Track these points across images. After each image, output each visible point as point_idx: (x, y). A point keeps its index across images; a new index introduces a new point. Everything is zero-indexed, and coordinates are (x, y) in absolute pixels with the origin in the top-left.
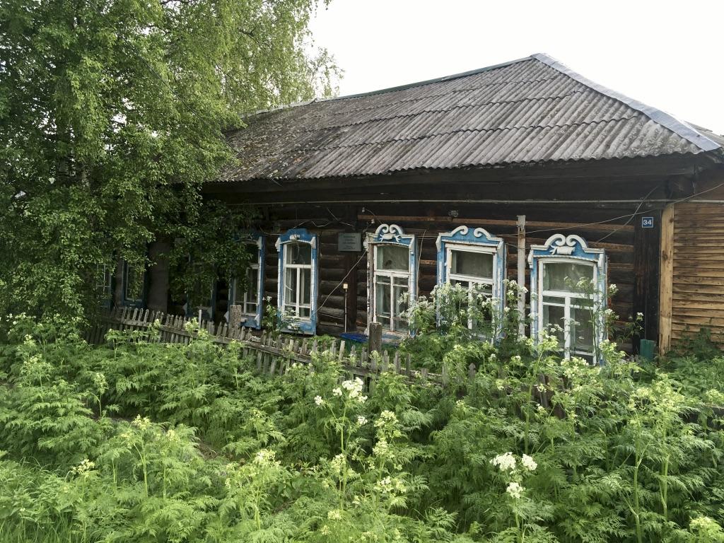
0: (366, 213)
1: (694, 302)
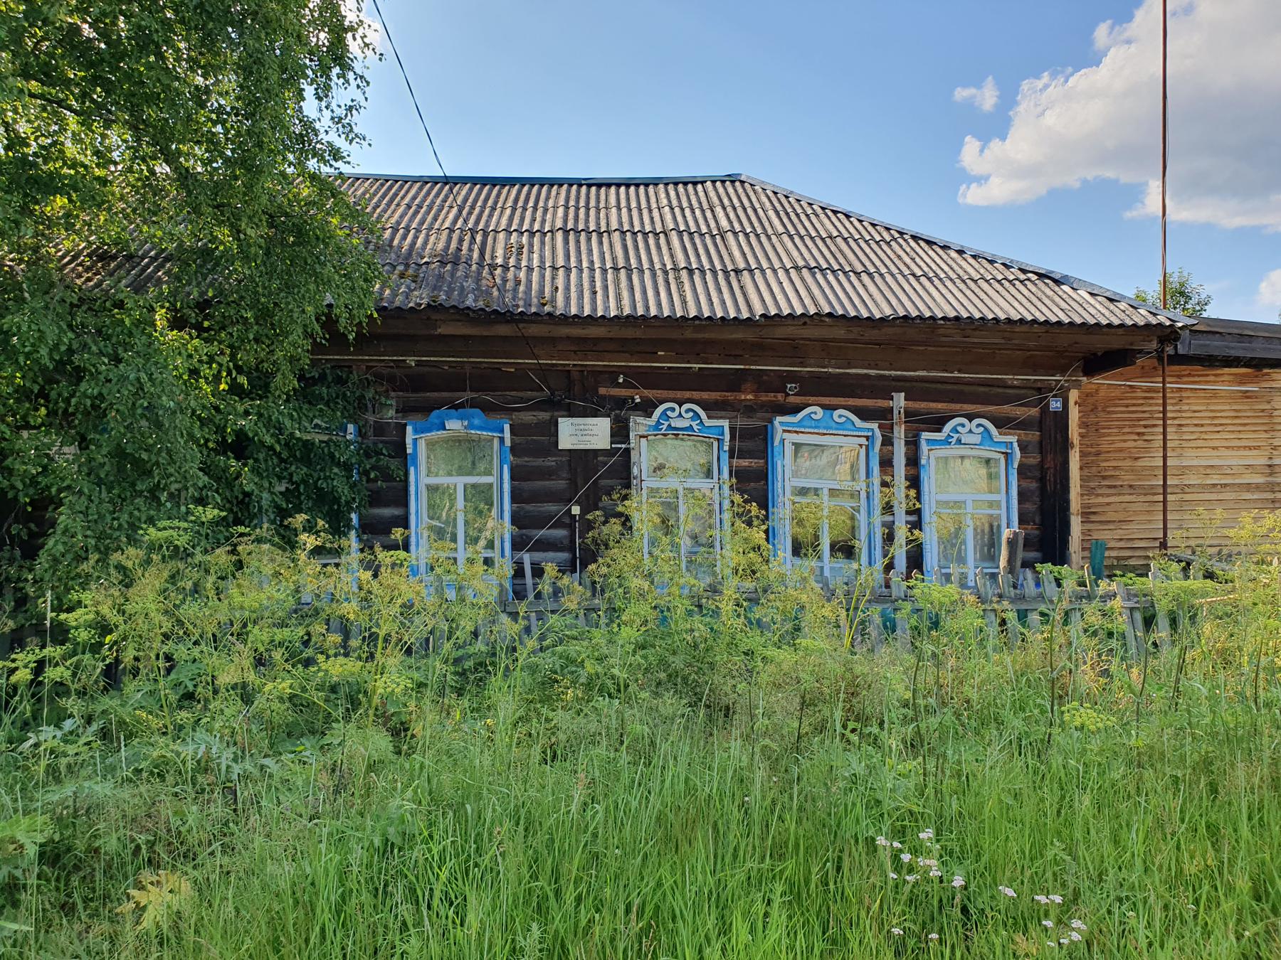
0: (626, 385)
1: (1098, 495)
